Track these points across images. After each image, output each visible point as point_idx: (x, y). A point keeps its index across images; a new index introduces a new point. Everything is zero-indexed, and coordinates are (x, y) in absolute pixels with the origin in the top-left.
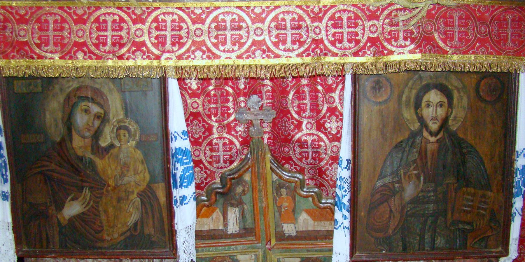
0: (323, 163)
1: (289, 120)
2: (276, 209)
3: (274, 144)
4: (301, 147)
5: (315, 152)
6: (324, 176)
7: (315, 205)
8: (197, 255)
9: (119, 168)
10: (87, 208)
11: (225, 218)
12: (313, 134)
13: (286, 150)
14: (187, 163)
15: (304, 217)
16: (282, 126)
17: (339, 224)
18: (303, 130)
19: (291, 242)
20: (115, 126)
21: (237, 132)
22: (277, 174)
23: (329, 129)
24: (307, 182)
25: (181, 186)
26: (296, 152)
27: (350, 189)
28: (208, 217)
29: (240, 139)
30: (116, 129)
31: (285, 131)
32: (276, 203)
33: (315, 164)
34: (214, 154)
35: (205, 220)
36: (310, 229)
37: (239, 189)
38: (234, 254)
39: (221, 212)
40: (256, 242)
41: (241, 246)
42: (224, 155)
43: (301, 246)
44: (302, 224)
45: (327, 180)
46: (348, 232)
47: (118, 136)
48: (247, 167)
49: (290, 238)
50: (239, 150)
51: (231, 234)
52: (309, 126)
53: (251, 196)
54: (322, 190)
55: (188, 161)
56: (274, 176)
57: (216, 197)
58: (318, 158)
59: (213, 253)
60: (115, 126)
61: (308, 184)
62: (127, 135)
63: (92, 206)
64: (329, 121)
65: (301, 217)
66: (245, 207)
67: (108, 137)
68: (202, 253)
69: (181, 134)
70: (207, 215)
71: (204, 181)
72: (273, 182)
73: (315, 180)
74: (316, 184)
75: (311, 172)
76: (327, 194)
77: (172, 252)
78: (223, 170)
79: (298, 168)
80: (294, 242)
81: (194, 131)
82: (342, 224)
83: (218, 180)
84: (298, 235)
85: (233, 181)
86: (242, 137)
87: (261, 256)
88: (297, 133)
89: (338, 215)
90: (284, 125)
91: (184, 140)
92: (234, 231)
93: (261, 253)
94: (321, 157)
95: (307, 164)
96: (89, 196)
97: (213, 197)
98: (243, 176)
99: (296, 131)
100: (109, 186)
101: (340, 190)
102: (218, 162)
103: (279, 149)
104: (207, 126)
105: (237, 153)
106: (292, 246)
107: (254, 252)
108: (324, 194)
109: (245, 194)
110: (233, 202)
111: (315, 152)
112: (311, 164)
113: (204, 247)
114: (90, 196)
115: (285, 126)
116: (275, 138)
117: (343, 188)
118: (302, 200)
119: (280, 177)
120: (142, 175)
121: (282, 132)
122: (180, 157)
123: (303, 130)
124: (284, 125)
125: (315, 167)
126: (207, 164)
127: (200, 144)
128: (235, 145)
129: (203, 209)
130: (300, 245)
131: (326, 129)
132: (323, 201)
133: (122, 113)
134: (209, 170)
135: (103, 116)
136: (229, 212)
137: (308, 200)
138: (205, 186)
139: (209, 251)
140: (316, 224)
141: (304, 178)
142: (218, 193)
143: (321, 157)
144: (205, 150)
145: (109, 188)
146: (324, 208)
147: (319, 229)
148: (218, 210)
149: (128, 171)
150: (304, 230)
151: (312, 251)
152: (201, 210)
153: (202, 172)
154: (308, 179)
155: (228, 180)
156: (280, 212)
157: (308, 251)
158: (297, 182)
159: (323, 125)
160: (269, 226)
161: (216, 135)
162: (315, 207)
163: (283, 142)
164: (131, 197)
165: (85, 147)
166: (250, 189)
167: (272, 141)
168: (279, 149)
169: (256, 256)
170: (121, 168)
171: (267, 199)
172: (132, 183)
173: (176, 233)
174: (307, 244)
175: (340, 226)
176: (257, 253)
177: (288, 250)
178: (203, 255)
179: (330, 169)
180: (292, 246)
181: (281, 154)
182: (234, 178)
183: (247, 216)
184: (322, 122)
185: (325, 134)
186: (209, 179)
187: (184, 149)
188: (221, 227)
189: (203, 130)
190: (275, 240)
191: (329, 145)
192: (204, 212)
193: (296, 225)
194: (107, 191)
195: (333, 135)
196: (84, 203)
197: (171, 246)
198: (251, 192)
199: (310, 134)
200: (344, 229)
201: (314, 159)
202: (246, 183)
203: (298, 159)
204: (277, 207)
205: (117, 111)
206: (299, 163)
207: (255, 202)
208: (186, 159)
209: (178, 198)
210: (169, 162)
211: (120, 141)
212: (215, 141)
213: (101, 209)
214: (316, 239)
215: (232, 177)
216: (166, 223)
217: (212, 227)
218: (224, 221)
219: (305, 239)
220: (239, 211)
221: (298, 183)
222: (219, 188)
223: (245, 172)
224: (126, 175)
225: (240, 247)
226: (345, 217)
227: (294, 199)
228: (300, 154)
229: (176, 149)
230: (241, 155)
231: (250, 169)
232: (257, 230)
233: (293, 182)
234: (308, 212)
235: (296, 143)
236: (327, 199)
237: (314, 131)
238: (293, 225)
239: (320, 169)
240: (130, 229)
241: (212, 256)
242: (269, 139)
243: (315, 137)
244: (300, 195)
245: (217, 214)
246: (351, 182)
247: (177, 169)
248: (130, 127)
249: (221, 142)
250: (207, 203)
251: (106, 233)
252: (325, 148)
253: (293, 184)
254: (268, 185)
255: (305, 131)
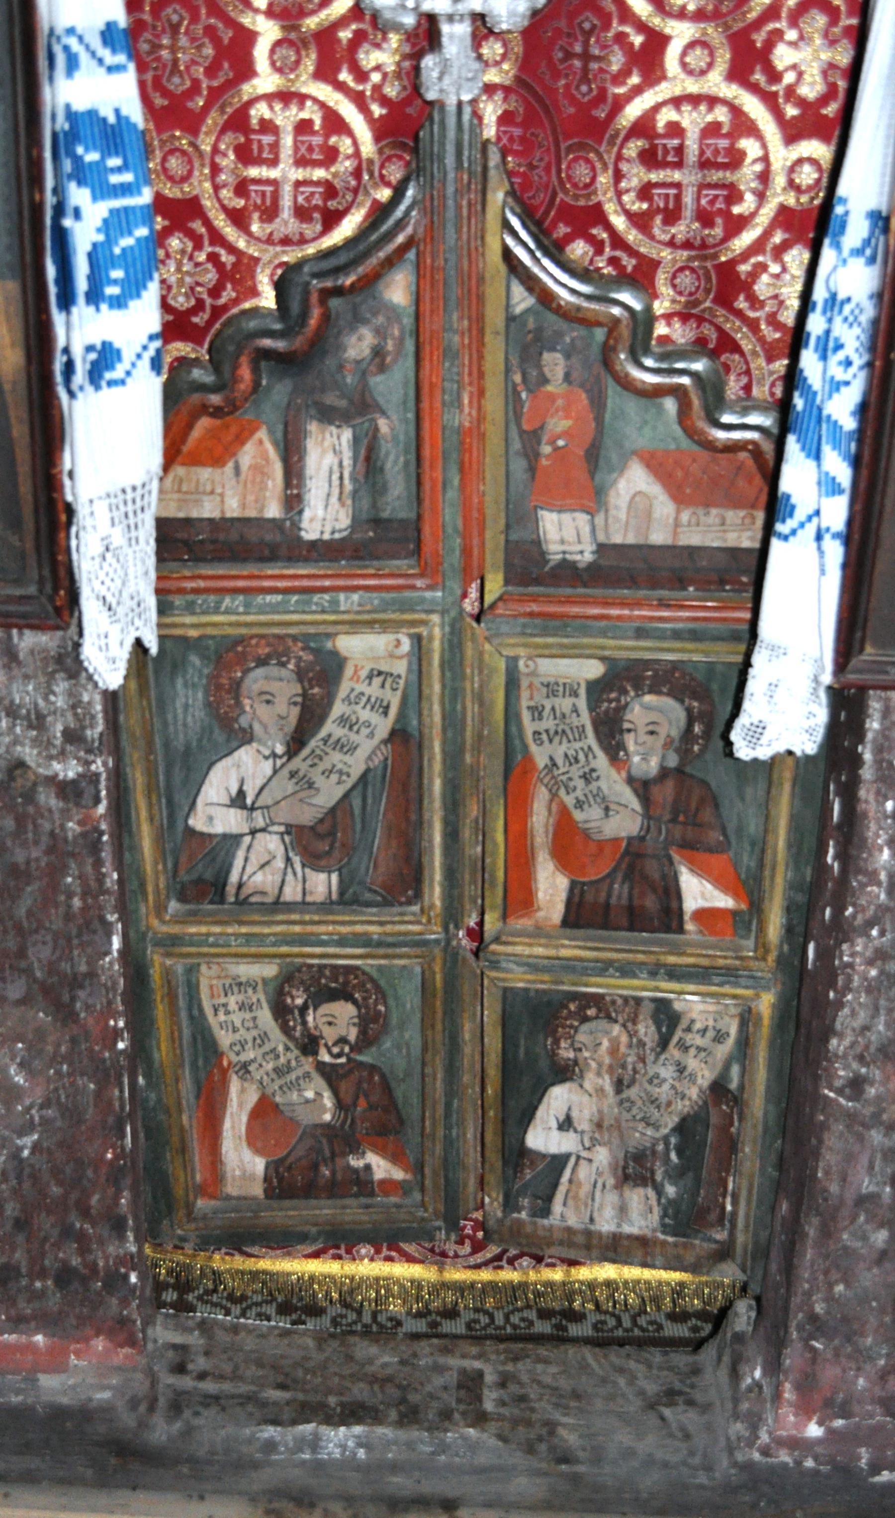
0: (747, 238)
1: (607, 26)
2: (517, 445)
3: (527, 146)
4: (649, 158)
5: (710, 186)
6: (741, 303)
7: (691, 432)
8: (160, 626)
11: (293, 473)
12: (712, 101)
13: (582, 172)
14: (125, 190)
15: (634, 483)
16: (569, 55)
17: (800, 514)
18: (663, 77)
19: (569, 591)
21: (361, 76)
22: (530, 282)
23: (789, 78)
24: (661, 329)
25: (94, 297)
26: (623, 185)
27: (866, 358)
28: (218, 461)
29: (377, 110)
31: (585, 78)
32: (518, 416)
33: (704, 246)
34: (254, 172)
35: (205, 474)
36: (658, 537)
37: (359, 345)
38: (321, 629)
39: (275, 444)
40: (419, 583)
41: (355, 597)
42: (298, 184)
43: (614, 612)
44: (623, 516)
45: (753, 325)
46: (835, 552)
48: (400, 239)
49: (568, 573)
50: (370, 162)
51: (313, 544)
52: (697, 58)
53: (411, 375)
54: (727, 368)
55: (128, 177)
56: (518, 291)
57: (256, 370)
58: (727, 215)
59: (233, 618)
61: (665, 340)
64: (791, 35)
65: (622, 485)
66: (383, 425)
68: (188, 620)
69: (96, 42)
70: (217, 454)
71: (208, 301)
72: (511, 319)
73: (700, 320)
74: (701, 342)
75: (686, 280)
76: (748, 388)
77: (51, 599)
78: (290, 256)
79: (629, 263)
80: (581, 590)
81: (165, 54)
82: (810, 518)
83: (268, 299)
84: (602, 562)
85: (335, 303)
86: (384, 101)
87: (436, 644)
88: (637, 91)
89: (798, 476)
90: (578, 48)
91: (110, 69)
92: (328, 529)
93: (437, 631)
94: (736, 210)
95: (671, 244)
97: (245, 372)
98: (381, 285)
99: (635, 80)
101: (824, 357)
102: (270, 213)
103: (548, 169)
104: (227, 35)
105: (357, 173)
106: (575, 610)
107: (413, 623)
108: (733, 387)
109: (382, 368)
110: (331, 399)
111: (710, 186)
112: (687, 245)
113: (196, 591)
115: (586, 57)
116: (530, 120)
117: (839, 347)
118: (632, 406)
119: (545, 297)
121: (567, 86)
122: (92, 157)
123: (663, 77)
124: (578, 48)
125: (704, 258)
126: (220, 221)
127: (192, 124)
128: (350, 133)
129: (194, 423)
130: (606, 604)
131: (775, 76)
132: (727, 419)
134: (232, 249)
136: (311, 444)
137: (660, 409)
138: (210, 323)
139: (216, 611)
140: (685, 516)
141: (648, 309)
142: (267, 354)
143: (736, 210)
144: (215, 150)
146: (733, 448)
147: (693, 539)
148: (262, 434)
150: (631, 540)
151: (661, 636)
152: (190, 426)
153: (202, 257)
154: (668, 317)
155: (314, 298)
156: (532, 456)
157: (641, 633)
158: (616, 321)
159: (764, 57)
160: (481, 511)
161: (266, 80)
162: (685, 443)
163: (568, 137)
166: (410, 346)
167: (517, 132)
168: (548, 169)
169: (417, 639)
171: (481, 393)
173: (69, 523)
174: (638, 604)
175: (802, 525)
176: (424, 631)
177: (557, 623)
178: (189, 624)
179: (775, 268)
180: (575, 610)
181: (554, 194)
182: (339, 291)
183: (388, 465)
184: (759, 39)
185: (770, 100)
186: (228, 293)
187: (112, 119)
188: (273, 511)
189: (209, 51)
190: (500, 577)
191: (781, 156)
192: (201, 440)
193: (599, 520)
195: (802, 103)
197: (46, 572)
198: (410, 362)
199: (695, 100)
200: (819, 537)
201: (705, 218)
202: (393, 312)
203: (630, 216)
204: (522, 432)
206: (632, 236)
207: (425, 405)
208: (119, 170)
209: (77, 352)
210: (37, 180)
212: (260, 111)
214: (680, 582)
215: (329, 284)
216: (24, 467)
217: (233, 508)
218: (288, 484)
219: (633, 581)
220: (356, 441)
221: (625, 331)
222: (271, 334)
223: (390, 263)
225: (349, 601)
226: (831, 487)
227: (598, 403)
228: (645, 192)
229: (71, 115)
230: (376, 186)
231: (411, 255)
232: (427, 531)
233: (599, 324)
234: (657, 465)
235: (627, 138)
236: (745, 411)
237: (716, 82)
238: (582, 519)
239: (727, 271)
241: (230, 631)
242: (505, 119)
243: (721, 114)
244: (627, 385)
245: (259, 450)
246: (875, 322)
247: (77, 214)
249: (286, 118)
250: (215, 399)
252: (758, 167)
253: (600, 334)
254: (488, 331)
255: (676, 81)
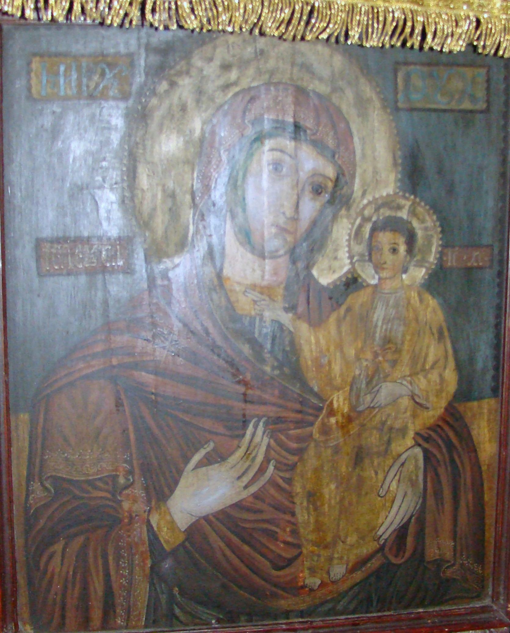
9: (369, 355)
10: (253, 489)
20: (366, 220)
30: (368, 228)
47: (372, 252)
60: (366, 220)
62: (402, 249)
63: (272, 482)
67: (343, 254)
96: (263, 448)
100: (332, 413)
114: (269, 446)
120: (434, 376)
133: (392, 177)
135: (330, 185)
145: (333, 420)
149: (394, 363)
164: (397, 447)
165: (267, 291)
170: (376, 355)
172: (405, 402)
194: (325, 431)
196: (243, 474)
205: (375, 172)
211: (378, 268)
213: (298, 488)
224: (386, 376)
240: (382, 549)
248: (415, 224)
251: (307, 564)
